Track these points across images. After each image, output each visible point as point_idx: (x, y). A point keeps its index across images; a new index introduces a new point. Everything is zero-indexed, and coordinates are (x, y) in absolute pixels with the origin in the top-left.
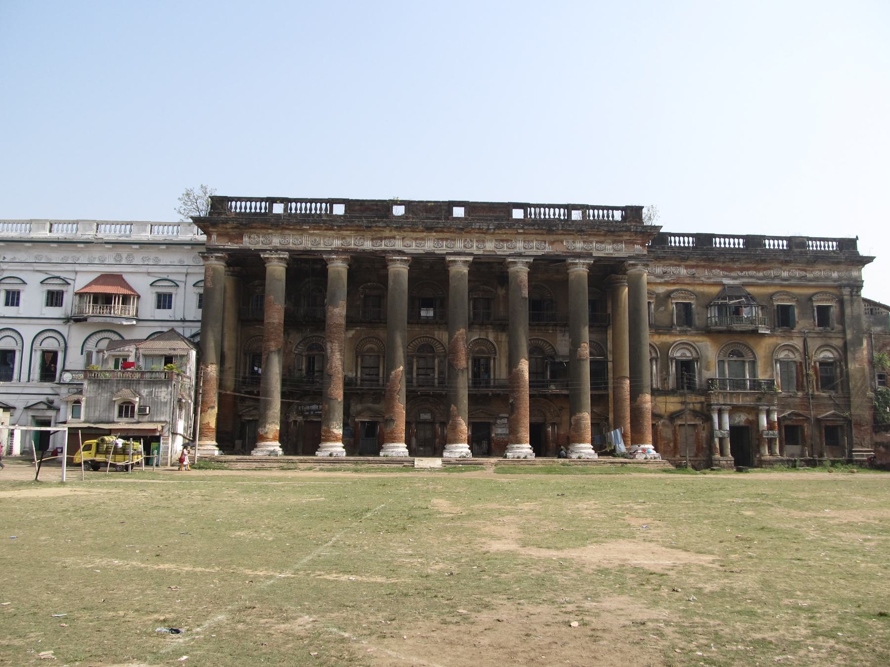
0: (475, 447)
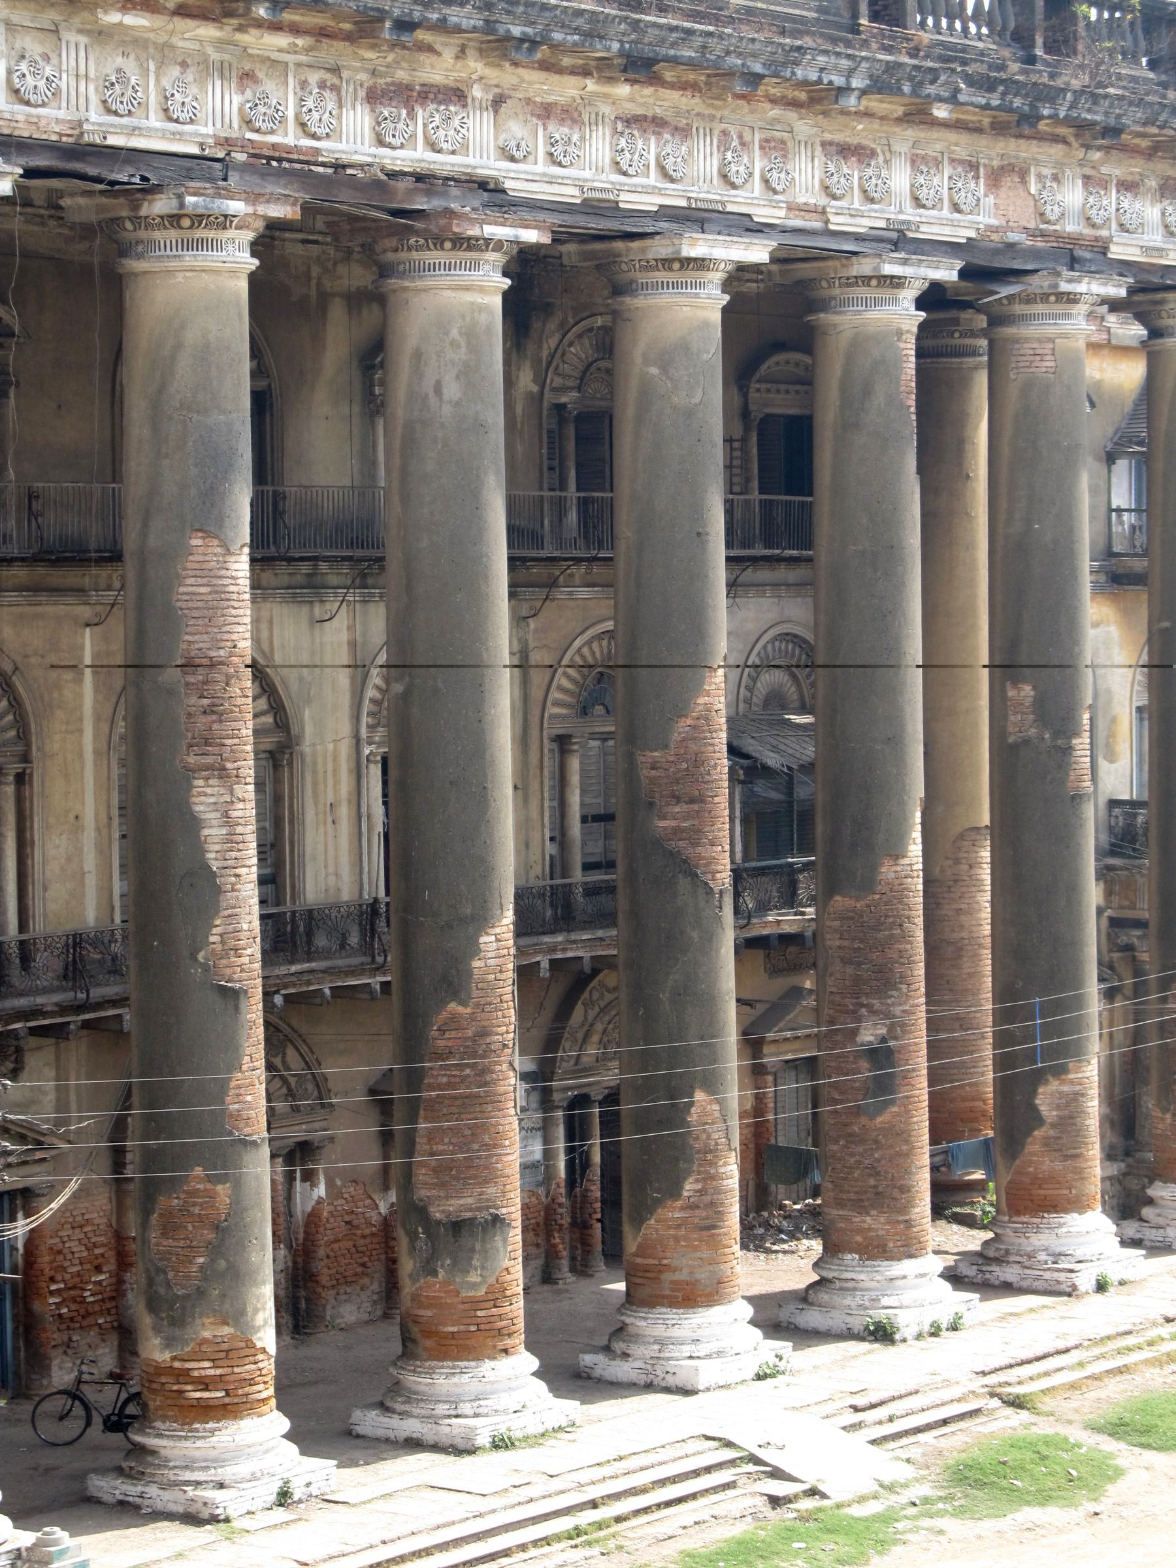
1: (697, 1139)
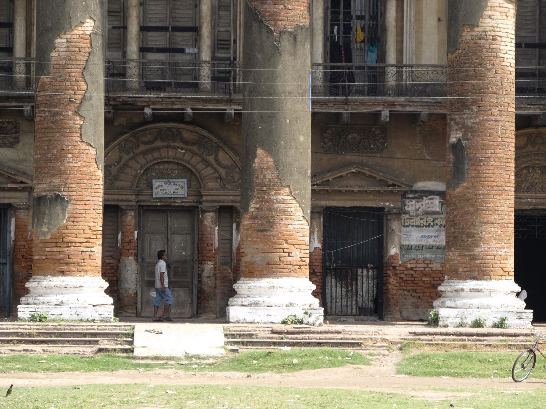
0: (335, 289)
1: (257, 177)
